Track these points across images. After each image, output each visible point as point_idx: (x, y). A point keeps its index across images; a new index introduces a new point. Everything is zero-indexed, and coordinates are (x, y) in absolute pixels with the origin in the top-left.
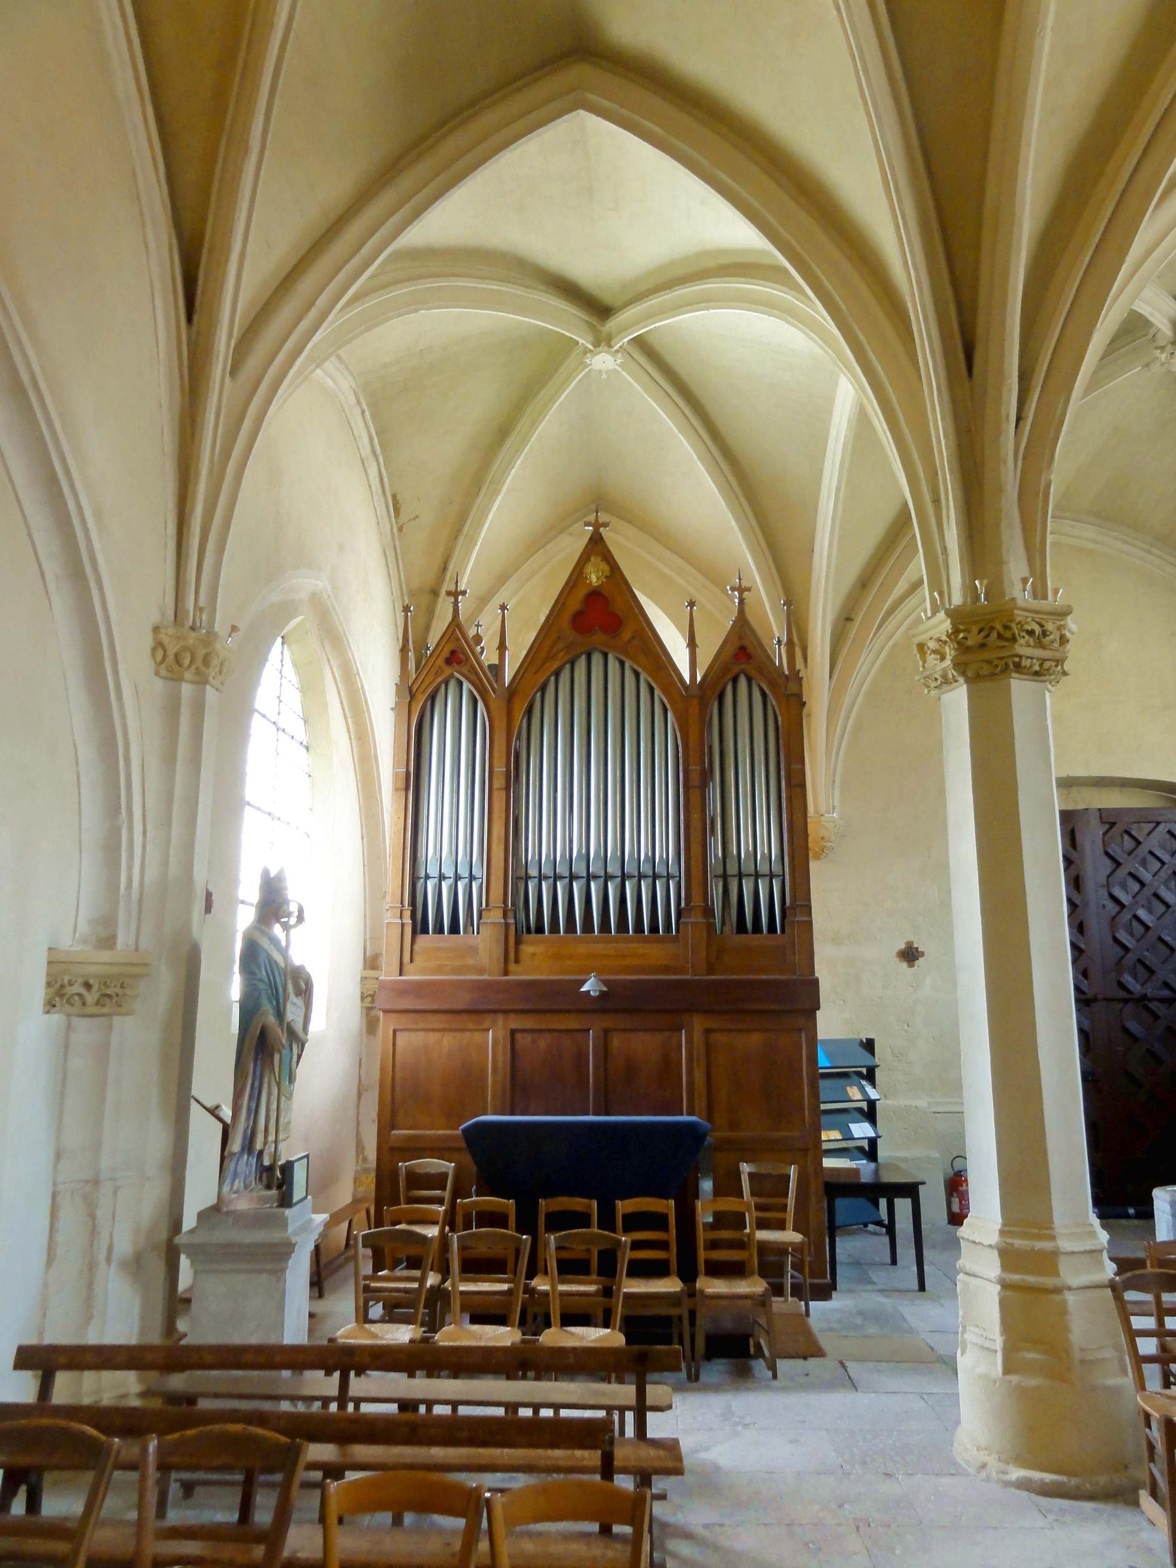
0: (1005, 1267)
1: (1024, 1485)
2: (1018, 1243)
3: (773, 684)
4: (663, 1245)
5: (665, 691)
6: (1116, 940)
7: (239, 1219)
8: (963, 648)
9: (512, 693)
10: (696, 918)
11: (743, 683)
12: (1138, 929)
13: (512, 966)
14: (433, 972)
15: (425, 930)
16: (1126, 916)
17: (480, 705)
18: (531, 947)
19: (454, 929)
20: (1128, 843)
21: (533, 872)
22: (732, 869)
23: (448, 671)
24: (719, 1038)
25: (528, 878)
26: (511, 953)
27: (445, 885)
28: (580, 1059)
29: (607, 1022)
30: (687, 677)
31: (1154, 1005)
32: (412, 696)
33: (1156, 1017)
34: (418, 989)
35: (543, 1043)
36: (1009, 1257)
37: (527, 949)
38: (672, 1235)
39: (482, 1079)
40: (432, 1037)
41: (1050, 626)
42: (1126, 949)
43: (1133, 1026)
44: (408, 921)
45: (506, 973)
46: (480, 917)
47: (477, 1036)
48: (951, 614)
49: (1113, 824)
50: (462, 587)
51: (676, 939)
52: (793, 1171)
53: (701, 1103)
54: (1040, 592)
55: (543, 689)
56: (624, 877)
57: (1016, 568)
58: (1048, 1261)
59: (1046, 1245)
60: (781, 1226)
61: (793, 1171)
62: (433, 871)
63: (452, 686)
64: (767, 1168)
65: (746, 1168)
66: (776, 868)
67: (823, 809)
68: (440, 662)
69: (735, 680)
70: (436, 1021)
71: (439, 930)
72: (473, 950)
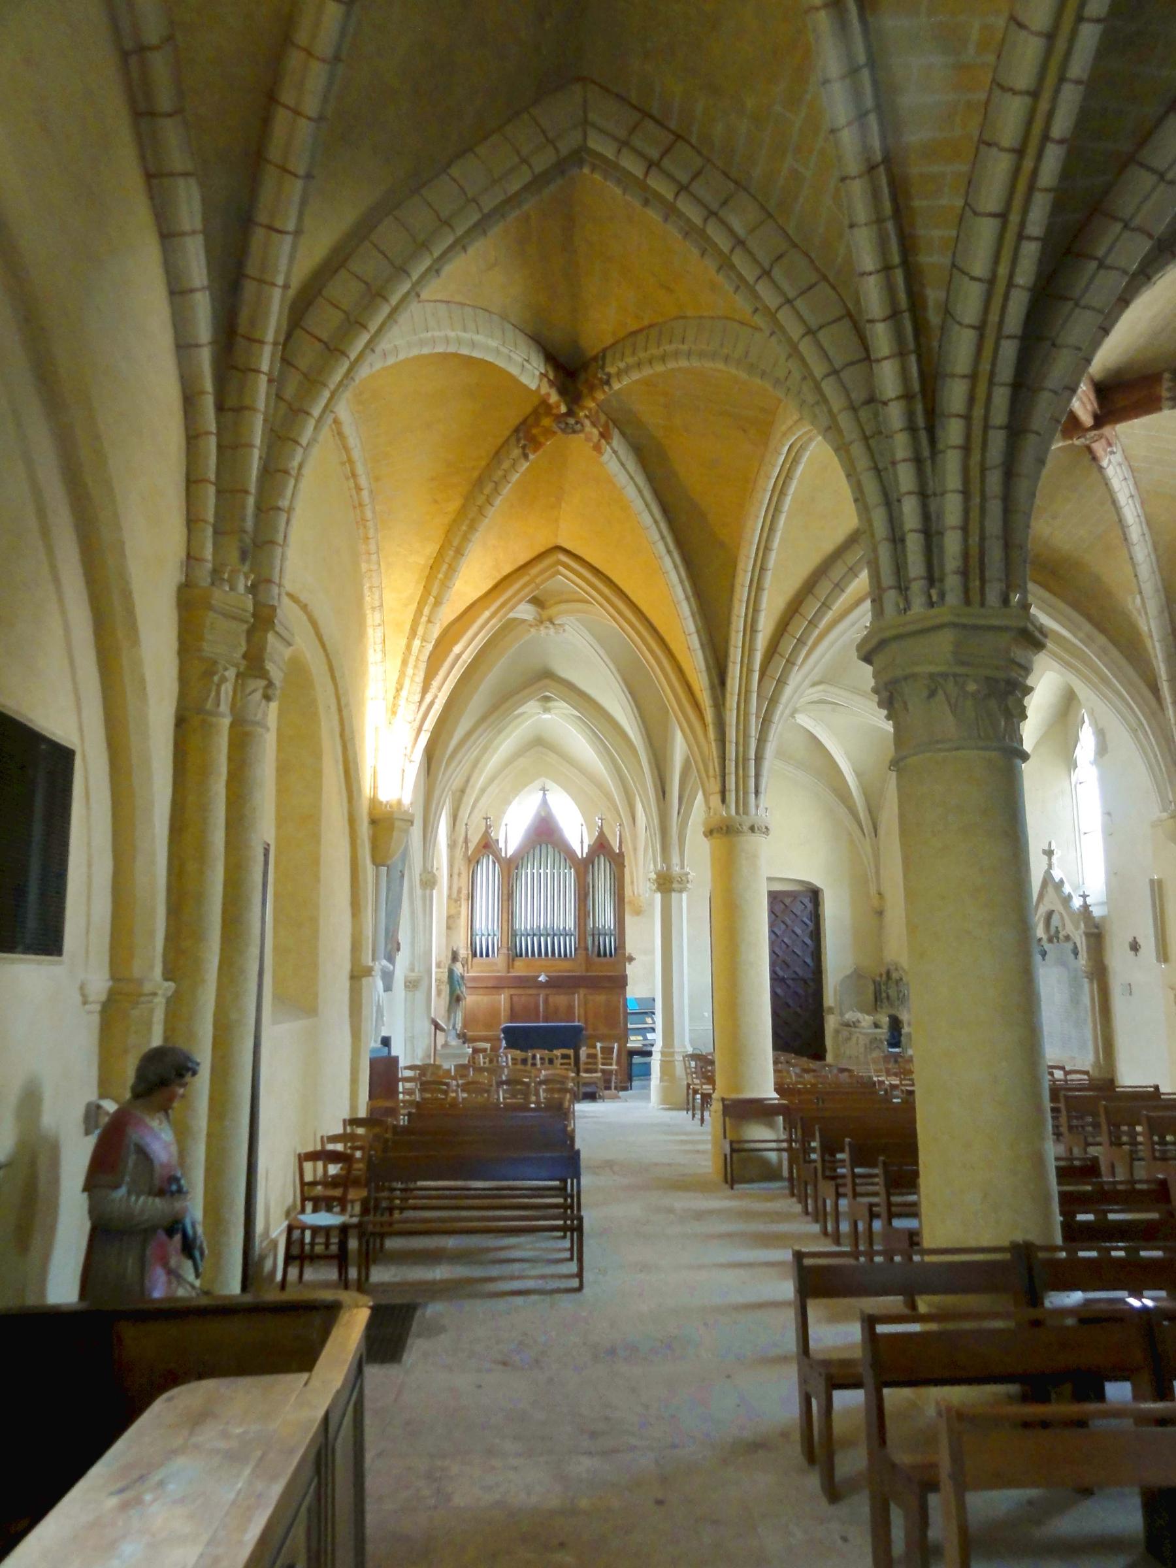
0: (662, 1056)
1: (663, 1109)
2: (666, 1050)
4: (569, 1064)
5: (570, 859)
7: (453, 1047)
10: (581, 952)
12: (784, 946)
13: (511, 970)
14: (482, 972)
16: (779, 940)
17: (497, 864)
18: (519, 963)
19: (487, 955)
20: (782, 906)
21: (519, 933)
22: (596, 932)
23: (484, 851)
24: (590, 997)
25: (516, 935)
26: (510, 963)
29: (548, 991)
30: (580, 857)
31: (789, 982)
32: (470, 861)
33: (789, 987)
34: (474, 979)
35: (523, 999)
36: (663, 1053)
38: (572, 1061)
39: (499, 1014)
40: (479, 998)
41: (683, 878)
42: (778, 956)
44: (470, 952)
45: (509, 972)
46: (498, 950)
47: (497, 997)
50: (489, 816)
51: (573, 960)
52: (616, 1046)
53: (583, 1019)
54: (682, 867)
57: (675, 860)
58: (672, 1054)
59: (671, 1050)
60: (611, 1065)
61: (616, 1046)
62: (479, 932)
63: (485, 856)
64: (606, 1044)
65: (599, 1045)
66: (613, 933)
67: (641, 892)
69: (598, 857)
70: (481, 991)
71: (481, 955)
72: (496, 964)
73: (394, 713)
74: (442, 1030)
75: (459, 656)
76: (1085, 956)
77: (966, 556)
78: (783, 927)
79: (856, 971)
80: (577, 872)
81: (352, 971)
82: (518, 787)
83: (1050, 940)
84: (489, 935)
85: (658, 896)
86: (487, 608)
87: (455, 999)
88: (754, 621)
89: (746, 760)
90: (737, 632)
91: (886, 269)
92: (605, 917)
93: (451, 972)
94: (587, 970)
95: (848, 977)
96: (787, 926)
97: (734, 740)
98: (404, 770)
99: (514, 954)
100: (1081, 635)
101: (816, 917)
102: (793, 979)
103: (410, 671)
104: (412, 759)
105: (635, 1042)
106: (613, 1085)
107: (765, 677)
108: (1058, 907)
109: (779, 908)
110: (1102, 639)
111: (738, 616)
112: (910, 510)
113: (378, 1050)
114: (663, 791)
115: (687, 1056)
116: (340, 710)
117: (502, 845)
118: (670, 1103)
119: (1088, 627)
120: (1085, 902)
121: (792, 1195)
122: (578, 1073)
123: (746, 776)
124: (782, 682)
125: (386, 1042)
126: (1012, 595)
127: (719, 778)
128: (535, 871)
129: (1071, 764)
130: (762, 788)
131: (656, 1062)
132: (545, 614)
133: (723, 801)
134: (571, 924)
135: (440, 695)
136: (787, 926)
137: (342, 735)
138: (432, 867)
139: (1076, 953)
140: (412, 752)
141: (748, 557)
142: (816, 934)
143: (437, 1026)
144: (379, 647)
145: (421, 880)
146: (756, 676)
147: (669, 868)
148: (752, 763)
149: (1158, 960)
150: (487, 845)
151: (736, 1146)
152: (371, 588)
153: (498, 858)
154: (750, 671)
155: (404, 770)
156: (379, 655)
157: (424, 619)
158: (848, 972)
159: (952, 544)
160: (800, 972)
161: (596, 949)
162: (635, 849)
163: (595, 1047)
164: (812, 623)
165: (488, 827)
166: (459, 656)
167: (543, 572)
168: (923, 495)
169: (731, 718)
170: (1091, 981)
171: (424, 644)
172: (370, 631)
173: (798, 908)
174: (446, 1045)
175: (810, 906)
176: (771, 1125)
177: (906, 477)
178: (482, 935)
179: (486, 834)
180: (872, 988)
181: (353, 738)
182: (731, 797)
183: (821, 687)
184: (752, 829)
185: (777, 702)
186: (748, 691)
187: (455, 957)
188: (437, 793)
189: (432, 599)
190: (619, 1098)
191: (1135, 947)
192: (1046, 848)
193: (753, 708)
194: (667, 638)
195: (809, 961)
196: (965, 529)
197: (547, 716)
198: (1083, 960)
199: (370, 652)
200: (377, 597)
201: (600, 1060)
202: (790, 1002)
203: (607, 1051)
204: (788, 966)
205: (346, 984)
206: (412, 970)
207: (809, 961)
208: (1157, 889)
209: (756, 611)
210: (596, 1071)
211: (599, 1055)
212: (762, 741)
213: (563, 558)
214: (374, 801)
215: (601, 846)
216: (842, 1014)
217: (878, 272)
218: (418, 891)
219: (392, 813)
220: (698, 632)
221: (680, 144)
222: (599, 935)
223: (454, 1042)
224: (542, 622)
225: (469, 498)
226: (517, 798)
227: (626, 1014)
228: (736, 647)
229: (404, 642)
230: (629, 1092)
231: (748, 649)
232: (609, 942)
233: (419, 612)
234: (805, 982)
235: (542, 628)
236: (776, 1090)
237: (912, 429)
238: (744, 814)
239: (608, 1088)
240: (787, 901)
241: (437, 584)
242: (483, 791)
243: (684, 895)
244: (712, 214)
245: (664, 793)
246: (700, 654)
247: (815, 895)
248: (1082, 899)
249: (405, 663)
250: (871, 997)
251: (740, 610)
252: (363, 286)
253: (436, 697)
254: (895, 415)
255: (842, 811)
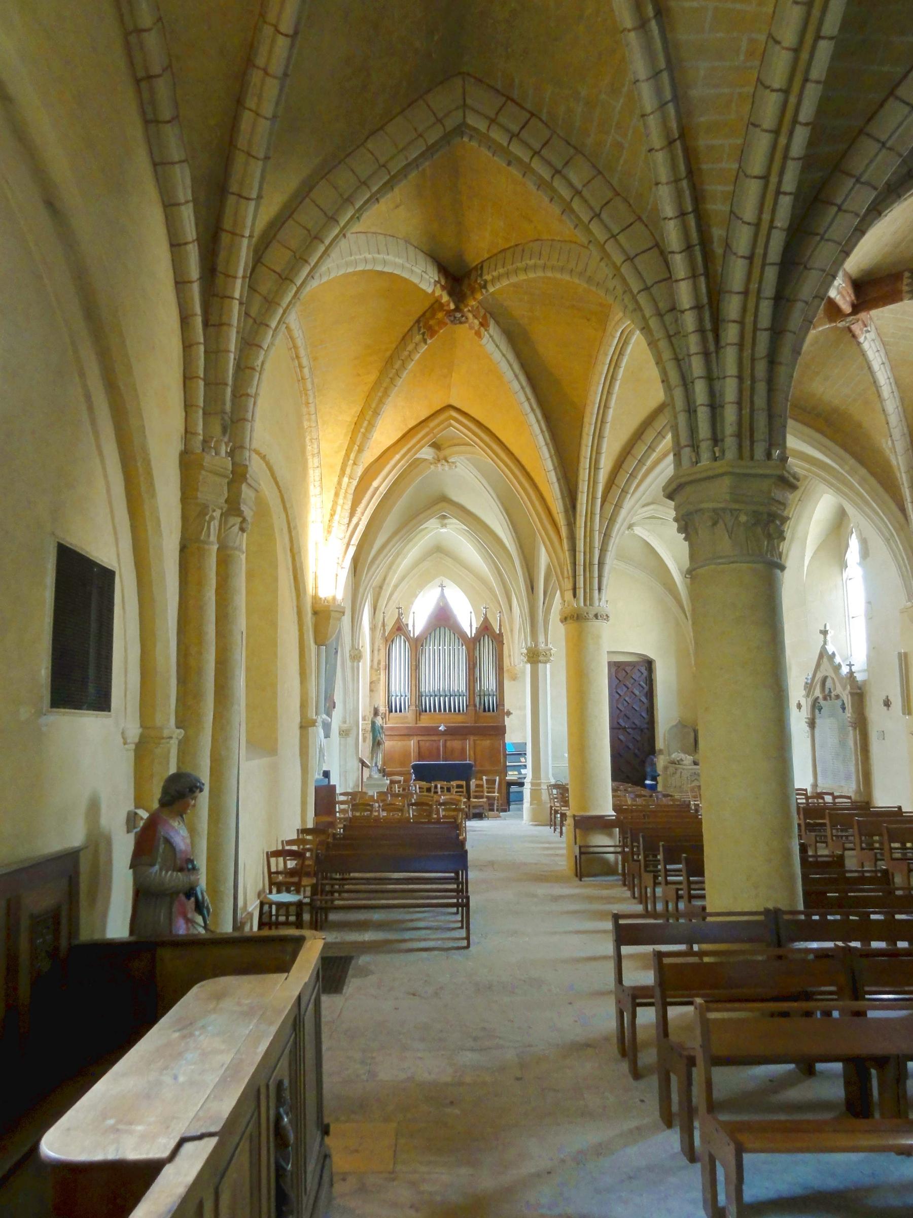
3: (495, 638)
4: (462, 792)
5: (462, 639)
6: (618, 708)
7: (376, 779)
8: (528, 657)
9: (417, 640)
10: (471, 708)
11: (486, 637)
12: (625, 702)
15: (392, 712)
19: (401, 711)
22: (482, 693)
23: (397, 633)
27: (398, 698)
28: (438, 749)
32: (387, 641)
33: (629, 733)
34: (392, 729)
35: (428, 744)
36: (532, 784)
37: (422, 717)
38: (464, 789)
43: (622, 737)
47: (407, 742)
48: (526, 649)
49: (619, 667)
51: (463, 714)
54: (547, 645)
55: (426, 639)
56: (450, 696)
57: (541, 639)
58: (539, 784)
65: (484, 778)
67: (516, 663)
68: (395, 630)
70: (396, 738)
71: (396, 711)
72: (406, 717)
73: (329, 532)
74: (367, 766)
75: (377, 489)
76: (850, 711)
77: (740, 423)
78: (625, 689)
79: (680, 721)
80: (468, 649)
81: (301, 722)
82: (422, 584)
83: (825, 699)
84: (401, 696)
85: (528, 666)
86: (397, 453)
87: (377, 744)
88: (597, 461)
89: (591, 564)
90: (585, 469)
91: (682, 214)
92: (489, 682)
93: (373, 723)
94: (476, 723)
95: (676, 726)
96: (628, 688)
97: (582, 549)
98: (337, 575)
99: (421, 711)
100: (847, 468)
101: (650, 681)
102: (634, 729)
103: (340, 501)
104: (343, 566)
105: (512, 776)
106: (495, 808)
107: (606, 503)
108: (831, 673)
109: (622, 675)
110: (863, 471)
111: (585, 458)
112: (700, 391)
113: (321, 780)
114: (531, 587)
115: (550, 786)
116: (290, 532)
117: (410, 628)
118: (537, 820)
119: (852, 461)
120: (851, 670)
121: (625, 885)
122: (469, 798)
123: (591, 577)
124: (618, 506)
125: (326, 774)
126: (773, 452)
127: (571, 579)
128: (436, 648)
129: (843, 565)
130: (604, 587)
131: (527, 791)
132: (442, 454)
133: (575, 595)
134: (463, 688)
135: (363, 518)
136: (628, 688)
137: (291, 550)
138: (359, 645)
139: (843, 708)
140: (343, 561)
141: (592, 414)
142: (650, 694)
143: (363, 764)
144: (317, 484)
145: (350, 655)
146: (599, 502)
147: (536, 645)
148: (596, 567)
149: (904, 714)
150: (400, 628)
151: (583, 850)
152: (311, 440)
153: (408, 638)
154: (594, 498)
155: (337, 575)
156: (318, 489)
157: (351, 462)
158: (674, 723)
159: (730, 415)
160: (637, 722)
161: (482, 707)
162: (512, 631)
163: (482, 779)
164: (641, 462)
165: (400, 614)
166: (377, 489)
167: (438, 425)
168: (710, 379)
169: (580, 533)
170: (855, 729)
171: (351, 481)
172: (311, 472)
173: (636, 675)
174: (370, 777)
175: (645, 673)
176: (610, 835)
177: (697, 366)
178: (397, 696)
179: (399, 620)
180: (692, 734)
181: (300, 552)
182: (580, 593)
183: (652, 507)
184: (596, 616)
185: (615, 521)
186: (593, 513)
187: (376, 713)
188: (361, 590)
189: (356, 447)
190: (500, 817)
191: (887, 703)
192: (823, 629)
193: (597, 527)
194: (533, 474)
195: (644, 714)
196: (739, 403)
197: (444, 530)
198: (849, 713)
199: (311, 488)
200: (315, 446)
201: (485, 789)
202: (631, 746)
203: (491, 782)
204: (628, 718)
205: (297, 732)
206: (345, 722)
207: (644, 714)
208: (903, 658)
209: (598, 453)
210: (482, 797)
211: (485, 785)
212: (603, 550)
213: (454, 414)
214: (315, 598)
215: (485, 629)
216: (669, 755)
217: (676, 217)
218: (348, 663)
219: (329, 606)
220: (555, 469)
221: (534, 121)
222: (484, 695)
223: (376, 776)
224: (439, 461)
225: (383, 372)
226: (422, 593)
227: (505, 755)
228: (584, 481)
229: (336, 479)
230: (508, 813)
231: (592, 482)
232: (492, 701)
233: (347, 456)
234: (642, 730)
235: (439, 465)
236: (614, 810)
237: (701, 330)
238: (590, 605)
239: (492, 810)
240: (628, 669)
241: (360, 435)
242: (396, 586)
243: (548, 665)
244: (557, 172)
245: (532, 588)
246: (556, 485)
247: (649, 664)
248: (848, 667)
249: (337, 495)
250: (692, 740)
251: (586, 452)
252: (306, 232)
253: (360, 519)
254: (689, 321)
255: (669, 599)
